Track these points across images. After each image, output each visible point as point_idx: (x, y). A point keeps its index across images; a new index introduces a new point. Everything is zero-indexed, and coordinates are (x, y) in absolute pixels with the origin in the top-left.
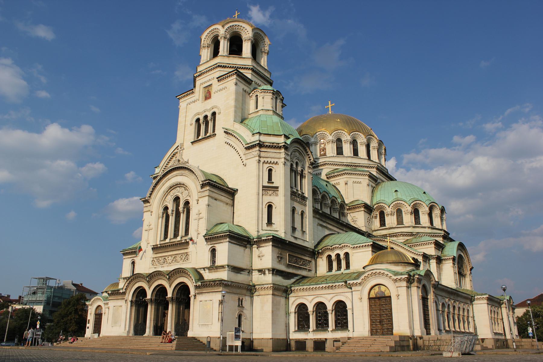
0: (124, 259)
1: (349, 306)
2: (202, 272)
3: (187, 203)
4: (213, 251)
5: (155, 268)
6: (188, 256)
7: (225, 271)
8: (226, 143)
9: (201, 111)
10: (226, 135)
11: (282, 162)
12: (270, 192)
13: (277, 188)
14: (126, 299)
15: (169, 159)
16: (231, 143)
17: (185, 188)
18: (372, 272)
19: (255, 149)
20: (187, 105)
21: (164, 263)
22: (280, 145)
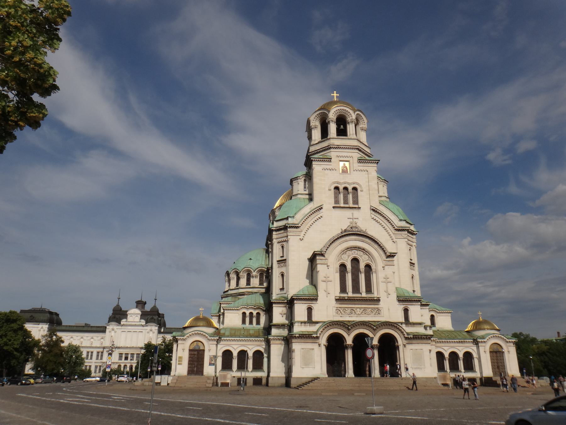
0: (296, 303)
1: (475, 355)
2: (400, 324)
3: (368, 267)
4: (406, 311)
5: (341, 316)
6: (379, 311)
7: (422, 327)
8: (373, 218)
9: (341, 182)
10: (373, 213)
11: (414, 246)
12: (412, 267)
13: (414, 264)
14: (320, 343)
15: (309, 214)
16: (379, 220)
17: (363, 252)
18: (493, 335)
19: (403, 233)
20: (323, 170)
21: (352, 313)
22: (414, 233)
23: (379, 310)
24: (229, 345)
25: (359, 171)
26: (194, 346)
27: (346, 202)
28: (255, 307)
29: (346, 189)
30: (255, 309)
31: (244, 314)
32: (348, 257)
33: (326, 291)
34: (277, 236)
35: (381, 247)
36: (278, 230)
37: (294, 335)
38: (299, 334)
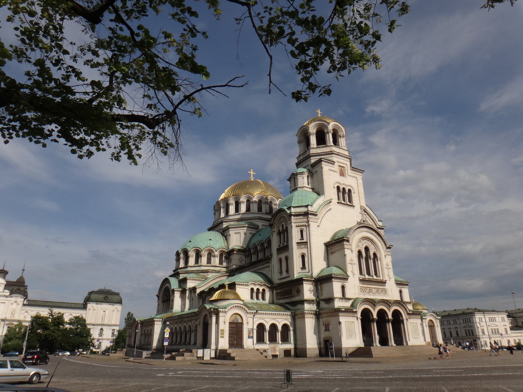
4: (401, 292)
9: (342, 182)
23: (386, 290)
24: (262, 319)
25: (352, 177)
26: (233, 319)
27: (344, 200)
28: (262, 283)
29: (344, 189)
30: (261, 285)
31: (252, 289)
32: (363, 245)
33: (352, 273)
34: (296, 221)
35: (383, 240)
36: (298, 215)
37: (341, 310)
38: (345, 309)
